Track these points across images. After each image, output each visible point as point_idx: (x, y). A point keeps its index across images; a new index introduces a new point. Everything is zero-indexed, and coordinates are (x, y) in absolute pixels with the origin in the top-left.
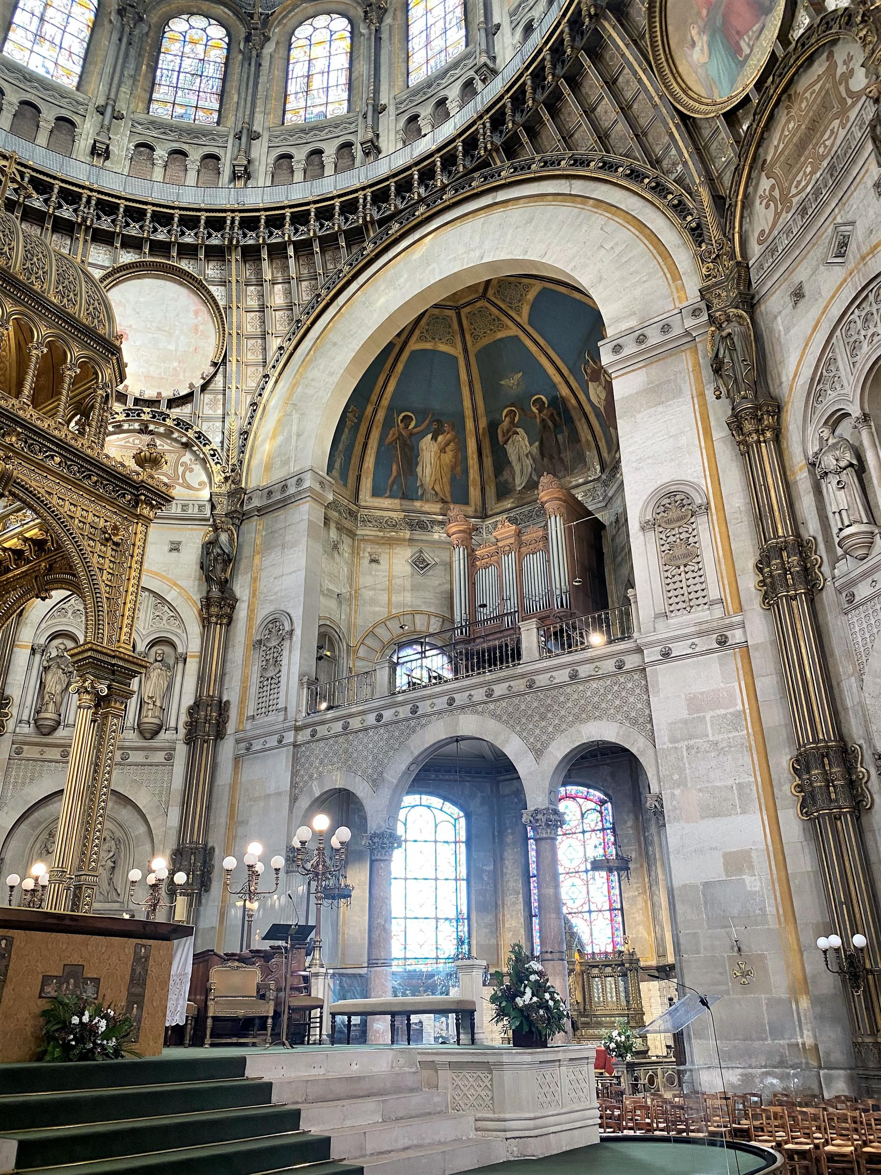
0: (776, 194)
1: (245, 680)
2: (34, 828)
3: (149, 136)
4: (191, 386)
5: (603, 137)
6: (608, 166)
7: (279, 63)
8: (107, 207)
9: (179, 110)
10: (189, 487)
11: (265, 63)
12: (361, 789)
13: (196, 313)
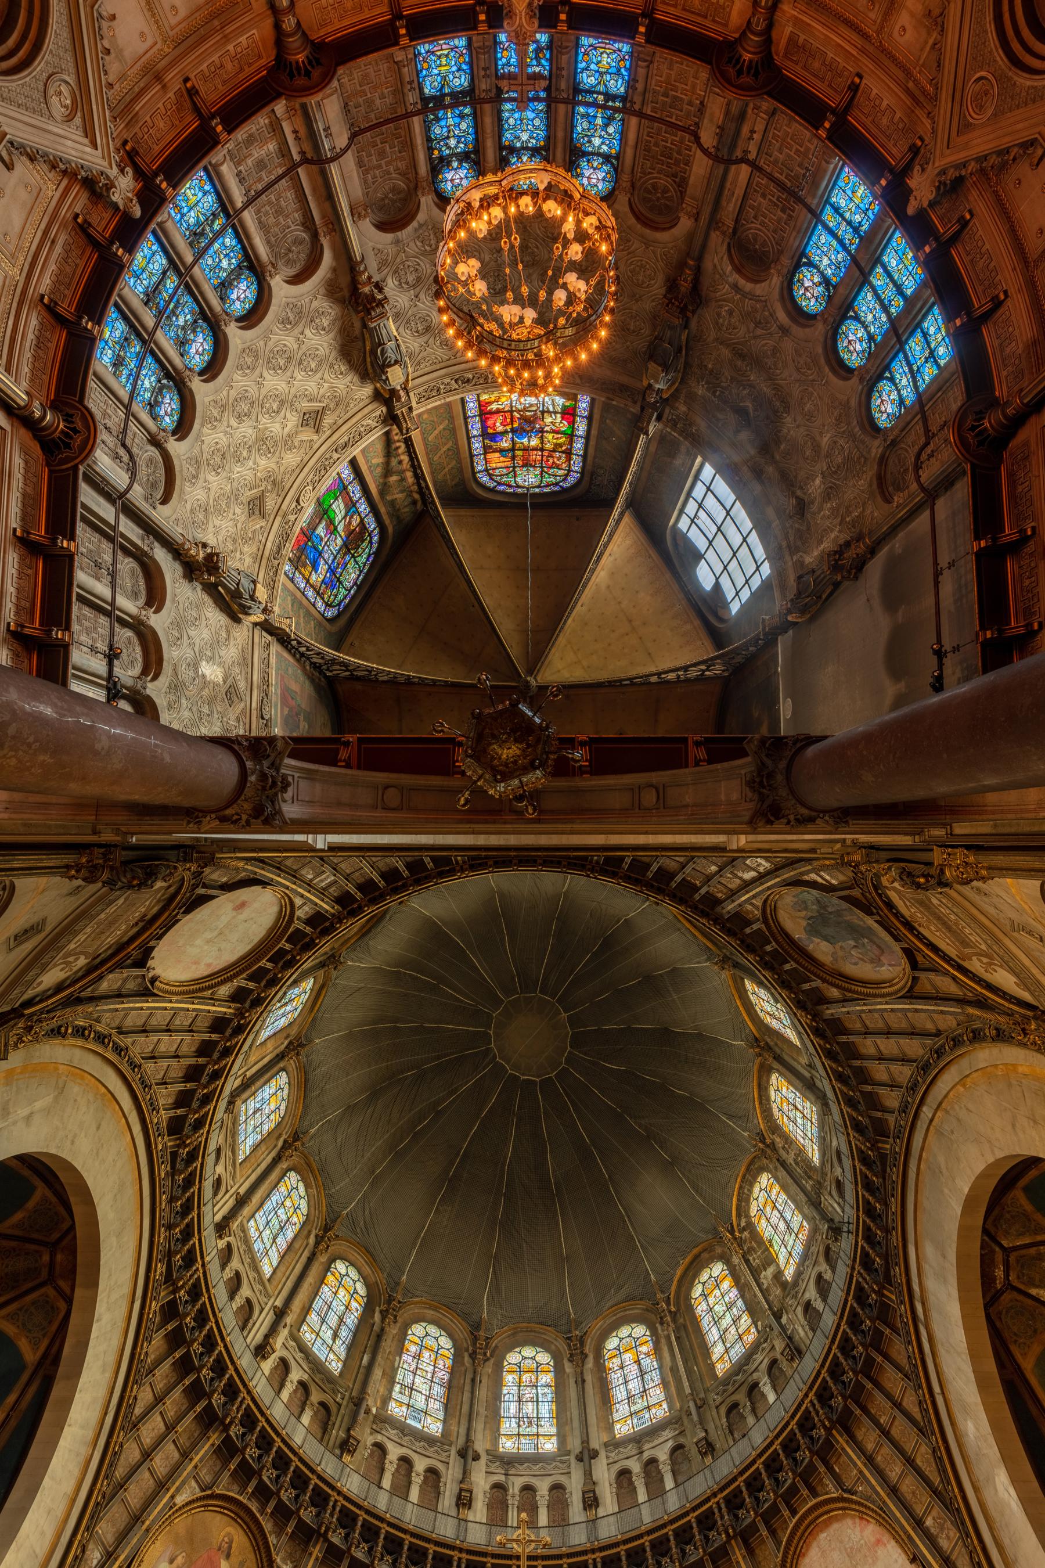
0: (985, 960)
5: (904, 1060)
6: (925, 1068)
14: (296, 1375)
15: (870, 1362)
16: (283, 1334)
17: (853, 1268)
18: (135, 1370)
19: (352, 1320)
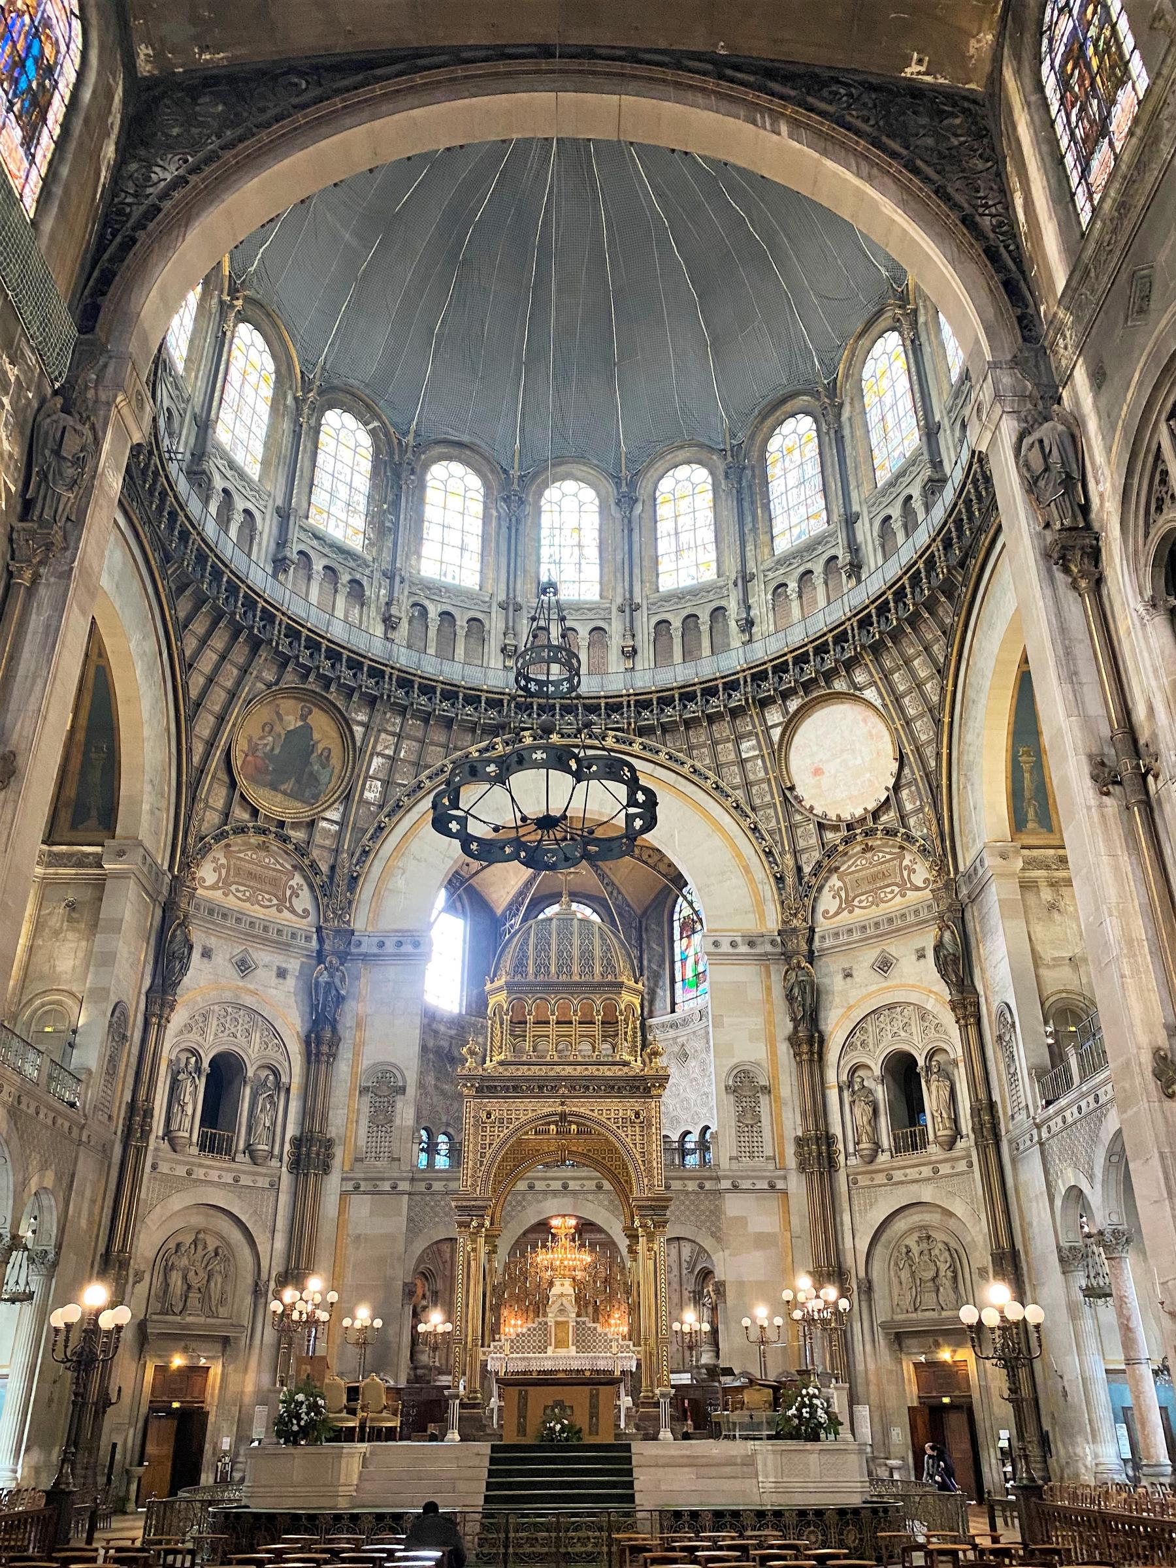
1: (1000, 1080)
2: (887, 1248)
3: (777, 576)
4: (887, 789)
7: (857, 420)
8: (759, 677)
9: (796, 531)
10: (918, 889)
11: (846, 432)
12: (1086, 1189)
13: (865, 720)
14: (318, 566)
15: (916, 614)
16: (294, 533)
17: (934, 540)
18: (171, 633)
19: (363, 483)
